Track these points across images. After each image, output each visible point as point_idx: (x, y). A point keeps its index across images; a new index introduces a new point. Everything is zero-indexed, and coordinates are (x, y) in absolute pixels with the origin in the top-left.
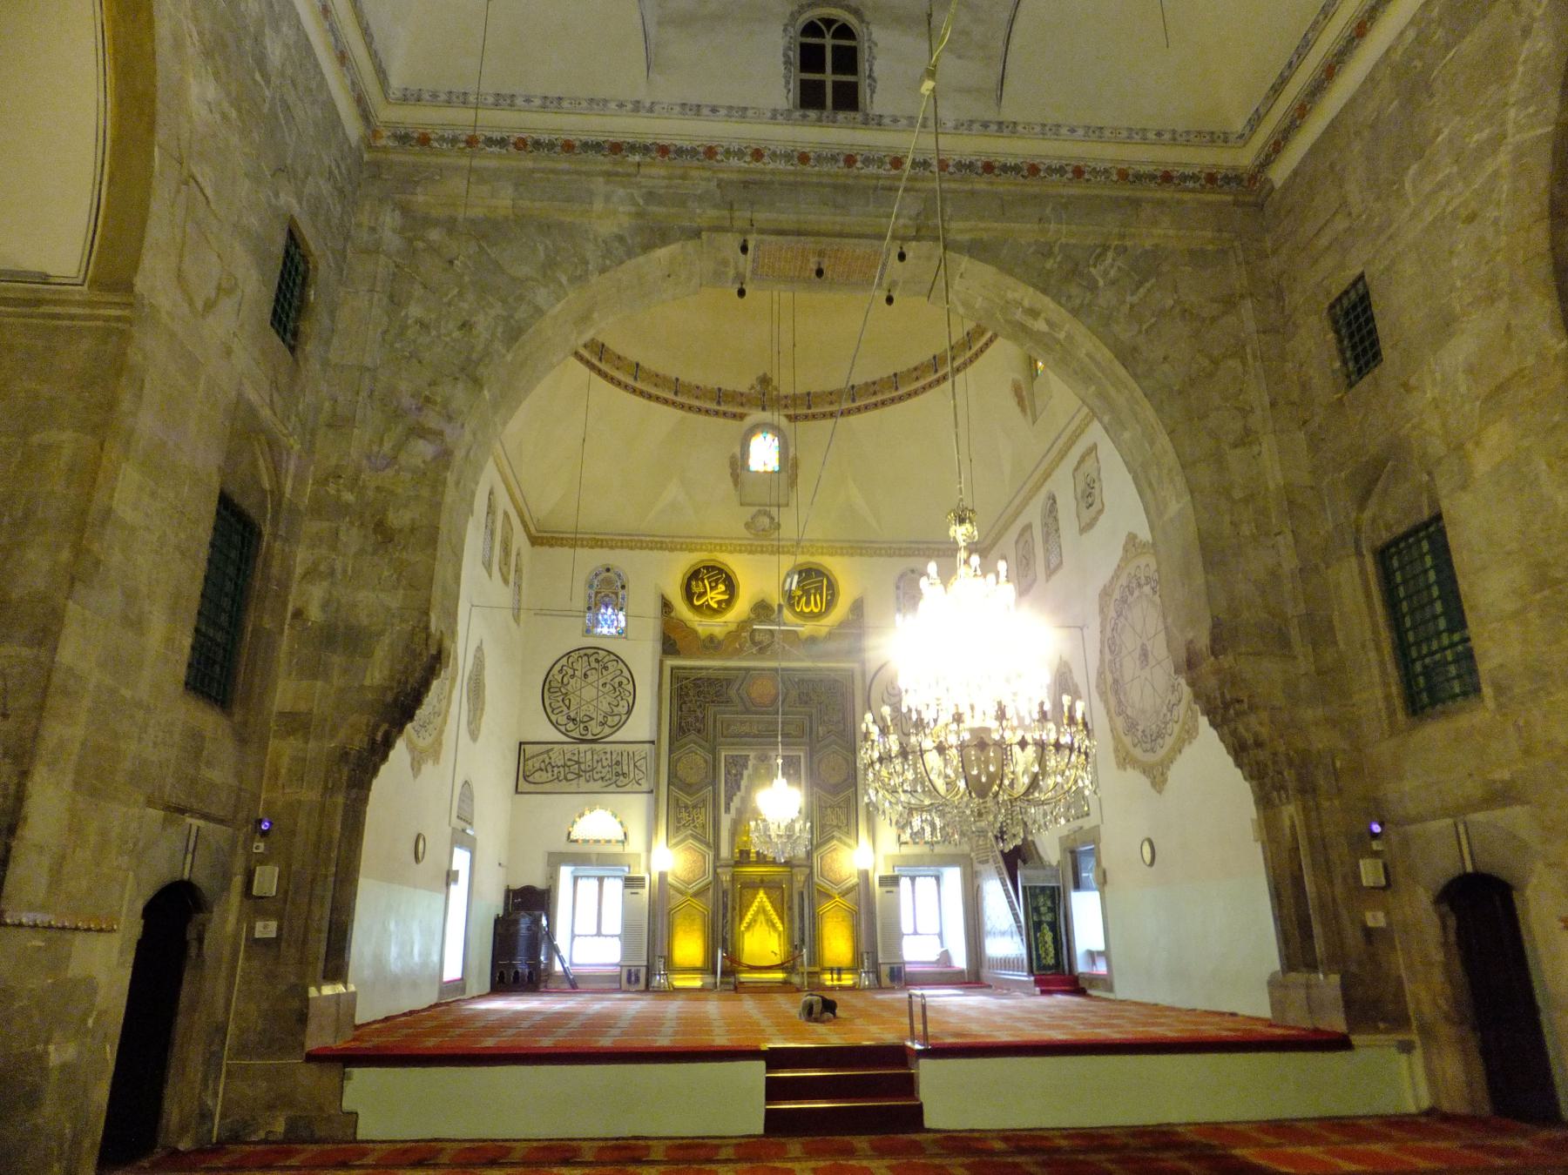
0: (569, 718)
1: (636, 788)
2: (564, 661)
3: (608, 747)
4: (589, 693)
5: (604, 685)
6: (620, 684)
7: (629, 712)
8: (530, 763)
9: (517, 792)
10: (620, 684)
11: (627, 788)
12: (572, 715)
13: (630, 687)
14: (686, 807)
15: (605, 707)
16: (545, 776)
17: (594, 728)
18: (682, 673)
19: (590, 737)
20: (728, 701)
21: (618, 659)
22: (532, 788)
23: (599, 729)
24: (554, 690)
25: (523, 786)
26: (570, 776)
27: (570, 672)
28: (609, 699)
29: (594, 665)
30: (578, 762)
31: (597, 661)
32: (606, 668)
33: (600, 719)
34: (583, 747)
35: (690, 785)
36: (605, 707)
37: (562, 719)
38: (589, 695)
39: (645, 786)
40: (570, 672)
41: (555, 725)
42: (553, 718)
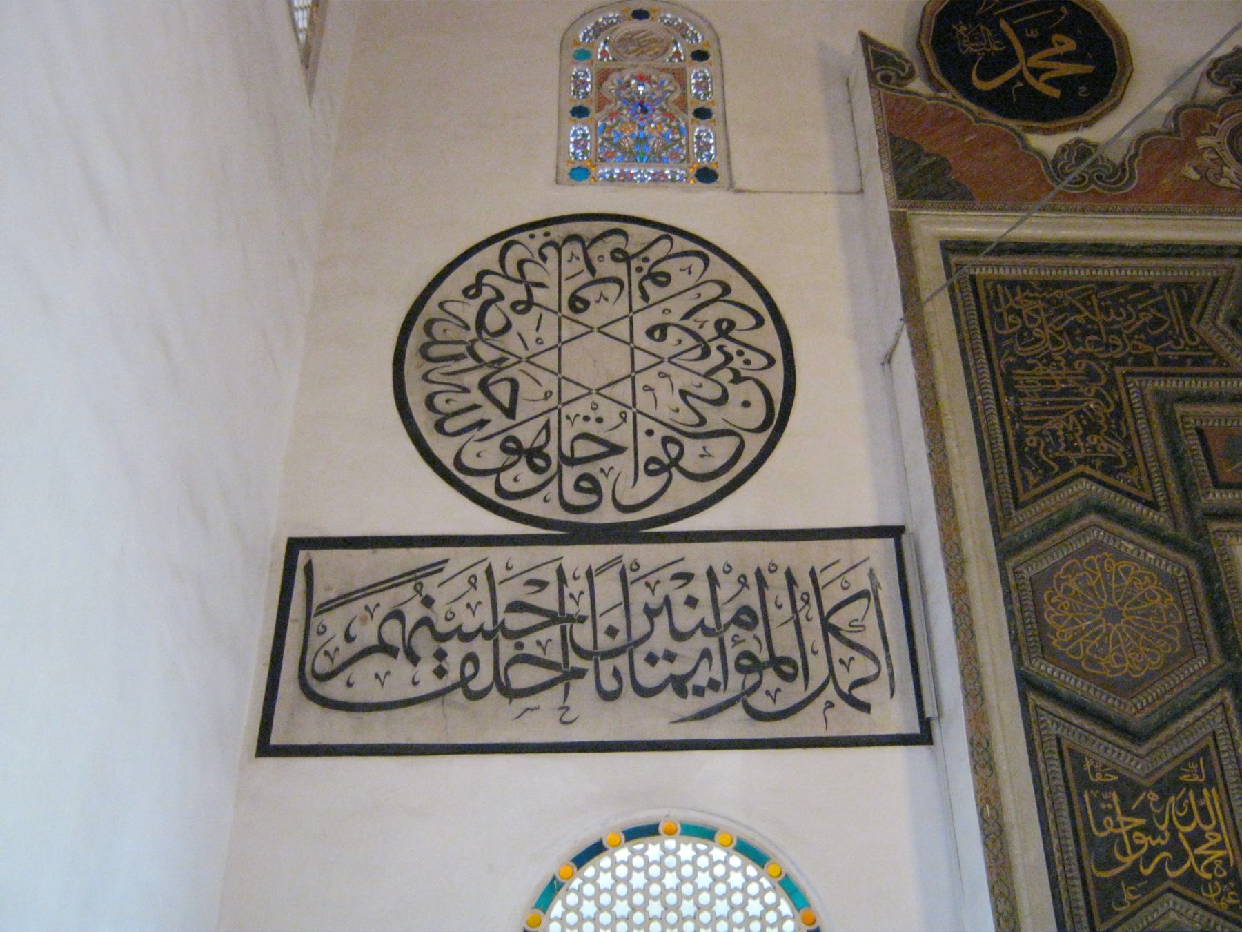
0: (513, 448)
1: (849, 722)
2: (488, 258)
3: (697, 557)
4: (595, 359)
5: (658, 331)
6: (724, 328)
7: (777, 420)
8: (335, 622)
9: (265, 748)
10: (724, 328)
11: (806, 724)
12: (527, 435)
13: (768, 338)
14: (1128, 789)
15: (667, 404)
16: (400, 678)
17: (626, 484)
18: (986, 269)
19: (607, 515)
20: (1204, 359)
21: (705, 249)
22: (341, 728)
23: (649, 486)
24: (447, 358)
25: (300, 721)
26: (523, 676)
27: (516, 292)
28: (683, 380)
29: (608, 268)
30: (553, 618)
31: (620, 256)
32: (662, 279)
33: (650, 448)
34: (577, 557)
35: (1124, 687)
36: (667, 404)
37: (492, 456)
38: (598, 371)
39: (894, 714)
40: (516, 292)
41: (452, 476)
42: (444, 449)
